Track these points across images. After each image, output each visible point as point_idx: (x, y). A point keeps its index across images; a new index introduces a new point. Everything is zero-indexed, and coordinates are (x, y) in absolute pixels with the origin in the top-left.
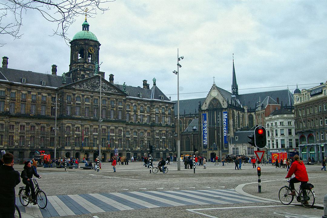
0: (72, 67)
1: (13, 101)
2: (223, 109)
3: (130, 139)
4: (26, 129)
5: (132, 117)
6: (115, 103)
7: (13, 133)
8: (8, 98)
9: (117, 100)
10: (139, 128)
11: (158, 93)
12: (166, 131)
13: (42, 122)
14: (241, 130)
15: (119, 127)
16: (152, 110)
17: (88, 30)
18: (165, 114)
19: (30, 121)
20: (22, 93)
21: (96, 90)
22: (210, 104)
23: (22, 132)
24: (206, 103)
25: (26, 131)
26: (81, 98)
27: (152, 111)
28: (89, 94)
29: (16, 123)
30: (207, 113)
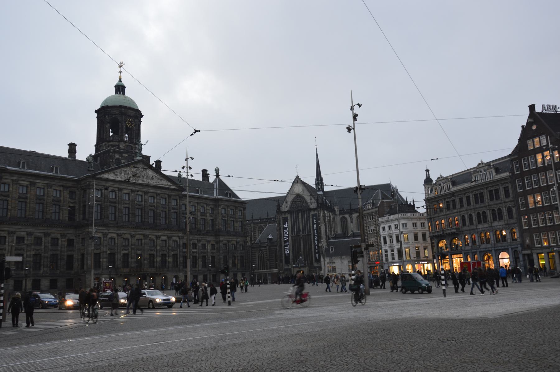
0: (100, 147)
1: (4, 198)
2: (311, 210)
7: (3, 249)
10: (199, 239)
11: (223, 188)
13: (53, 231)
14: (336, 237)
15: (173, 236)
17: (123, 94)
19: (33, 230)
21: (140, 182)
22: (292, 203)
24: (286, 203)
28: (129, 188)
29: (10, 233)
30: (289, 216)
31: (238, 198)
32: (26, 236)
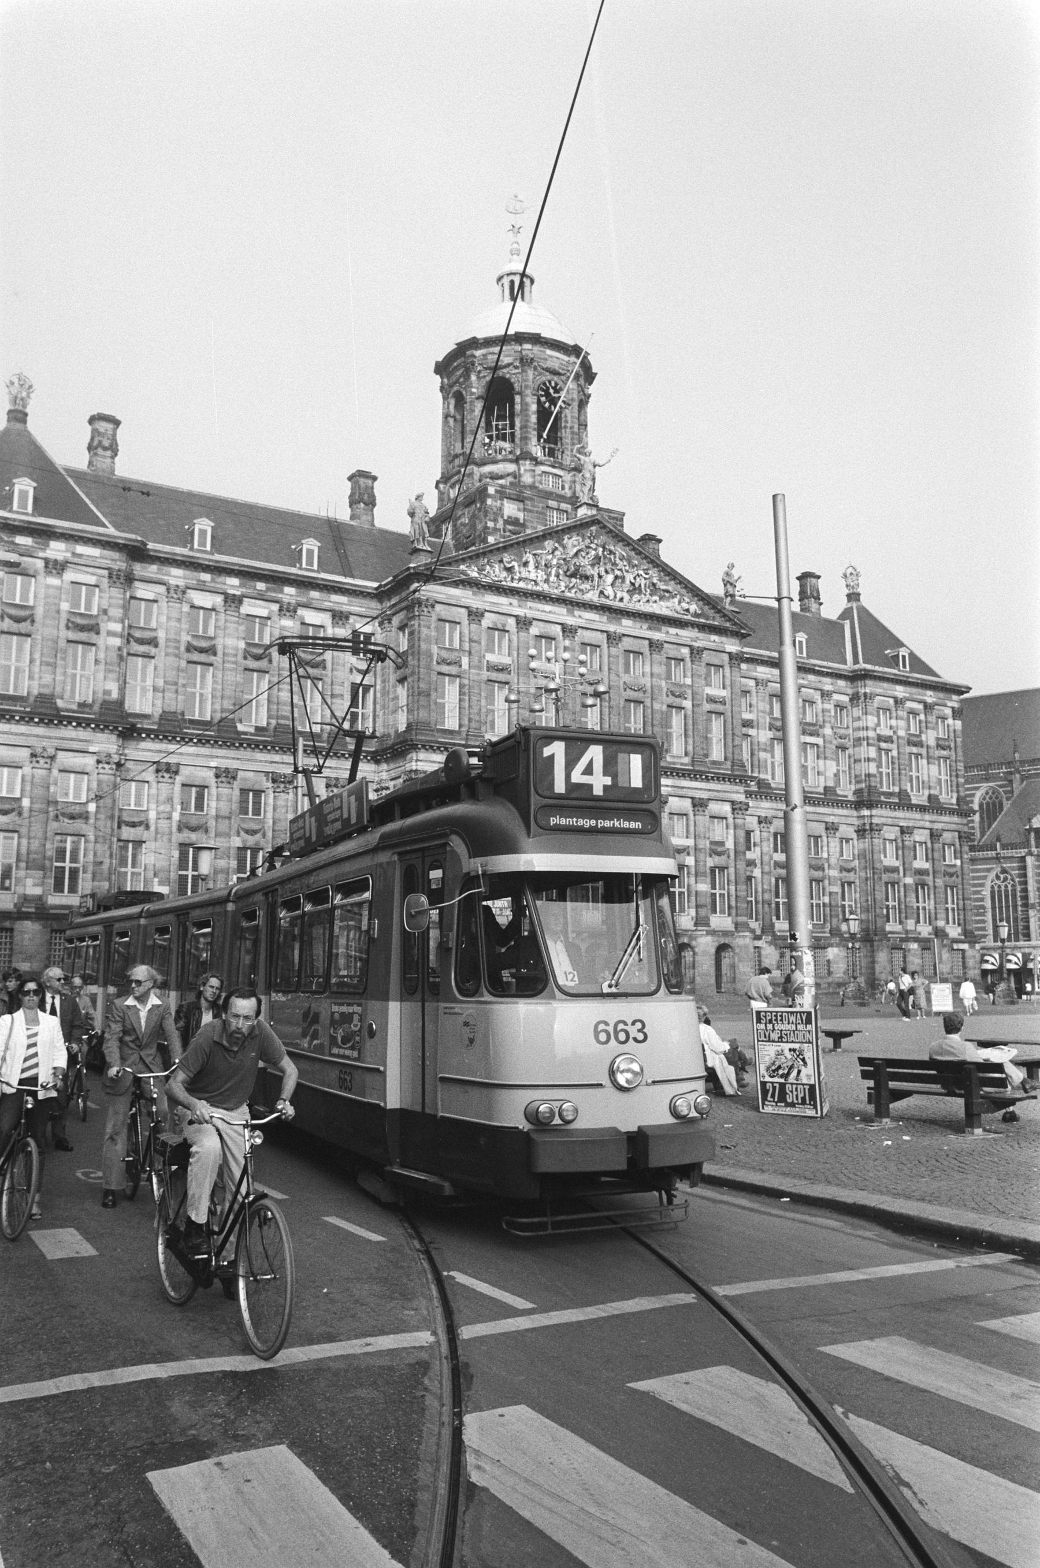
3: (757, 872)
4: (213, 804)
5: (763, 755)
6: (689, 674)
7: (140, 823)
8: (117, 627)
9: (696, 653)
12: (931, 829)
16: (859, 719)
18: (919, 744)
20: (193, 607)
21: (592, 596)
23: (194, 822)
25: (217, 817)
26: (515, 638)
27: (857, 724)
31: (930, 672)
32: (212, 781)
